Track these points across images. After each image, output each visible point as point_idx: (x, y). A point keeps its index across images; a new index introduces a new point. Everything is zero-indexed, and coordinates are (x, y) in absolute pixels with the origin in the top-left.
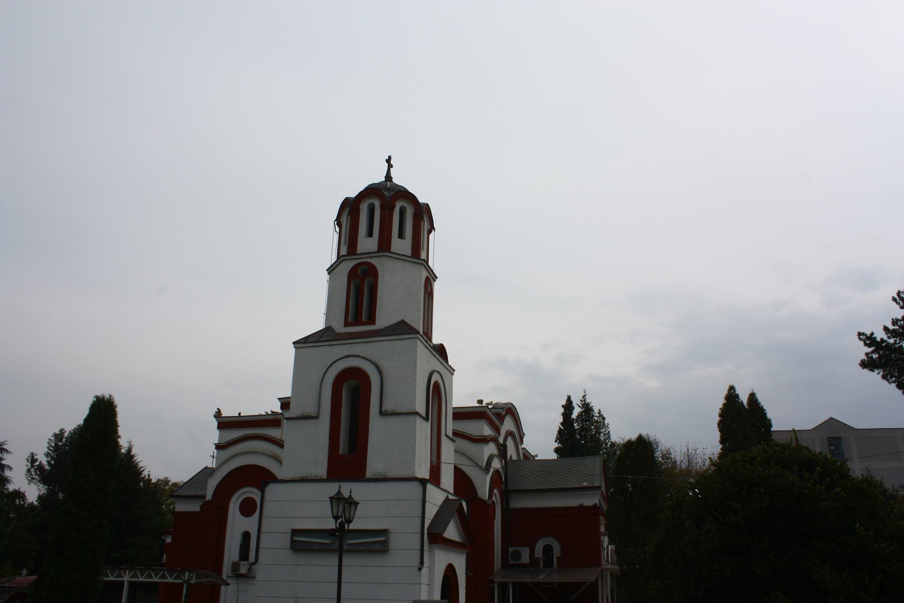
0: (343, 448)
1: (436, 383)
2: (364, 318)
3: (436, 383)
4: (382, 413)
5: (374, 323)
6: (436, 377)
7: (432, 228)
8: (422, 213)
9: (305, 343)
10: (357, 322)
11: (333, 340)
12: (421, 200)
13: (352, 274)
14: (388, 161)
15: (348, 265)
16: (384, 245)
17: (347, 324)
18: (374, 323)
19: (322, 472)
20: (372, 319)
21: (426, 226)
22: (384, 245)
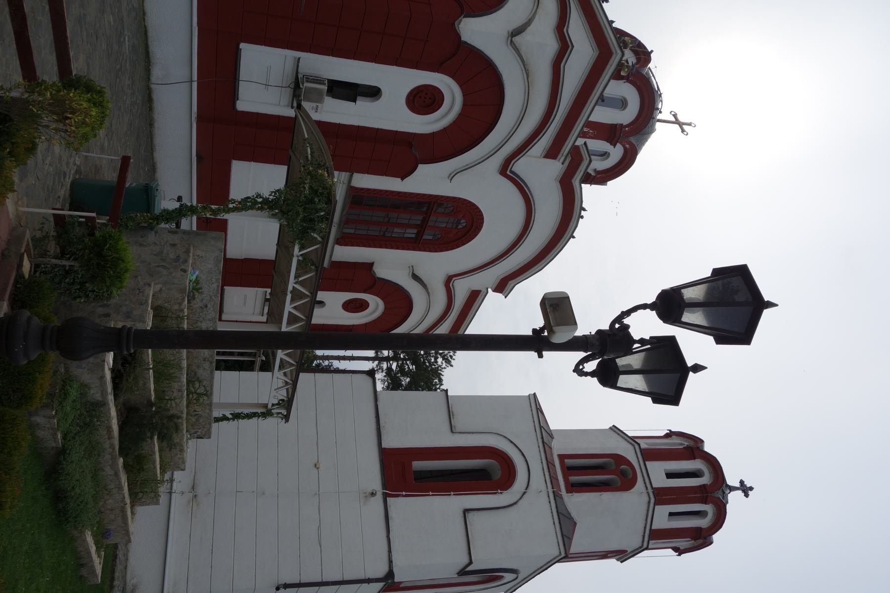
0: (418, 465)
1: (502, 577)
2: (574, 479)
3: (502, 577)
4: (466, 511)
5: (568, 491)
6: (508, 577)
7: (680, 551)
8: (700, 538)
9: (537, 409)
10: (568, 470)
11: (543, 442)
12: (715, 537)
13: (619, 459)
14: (751, 489)
15: (630, 454)
16: (662, 496)
17: (562, 457)
18: (568, 491)
19: (390, 442)
20: (573, 488)
21: (683, 543)
22: (662, 496)
